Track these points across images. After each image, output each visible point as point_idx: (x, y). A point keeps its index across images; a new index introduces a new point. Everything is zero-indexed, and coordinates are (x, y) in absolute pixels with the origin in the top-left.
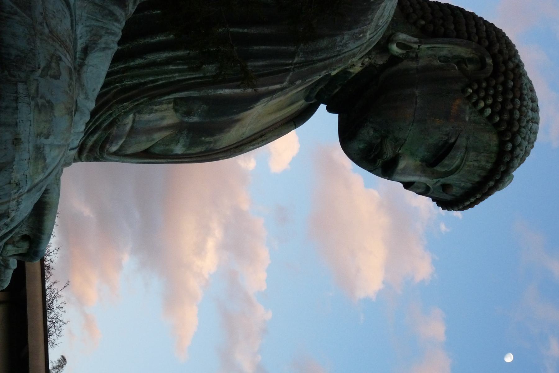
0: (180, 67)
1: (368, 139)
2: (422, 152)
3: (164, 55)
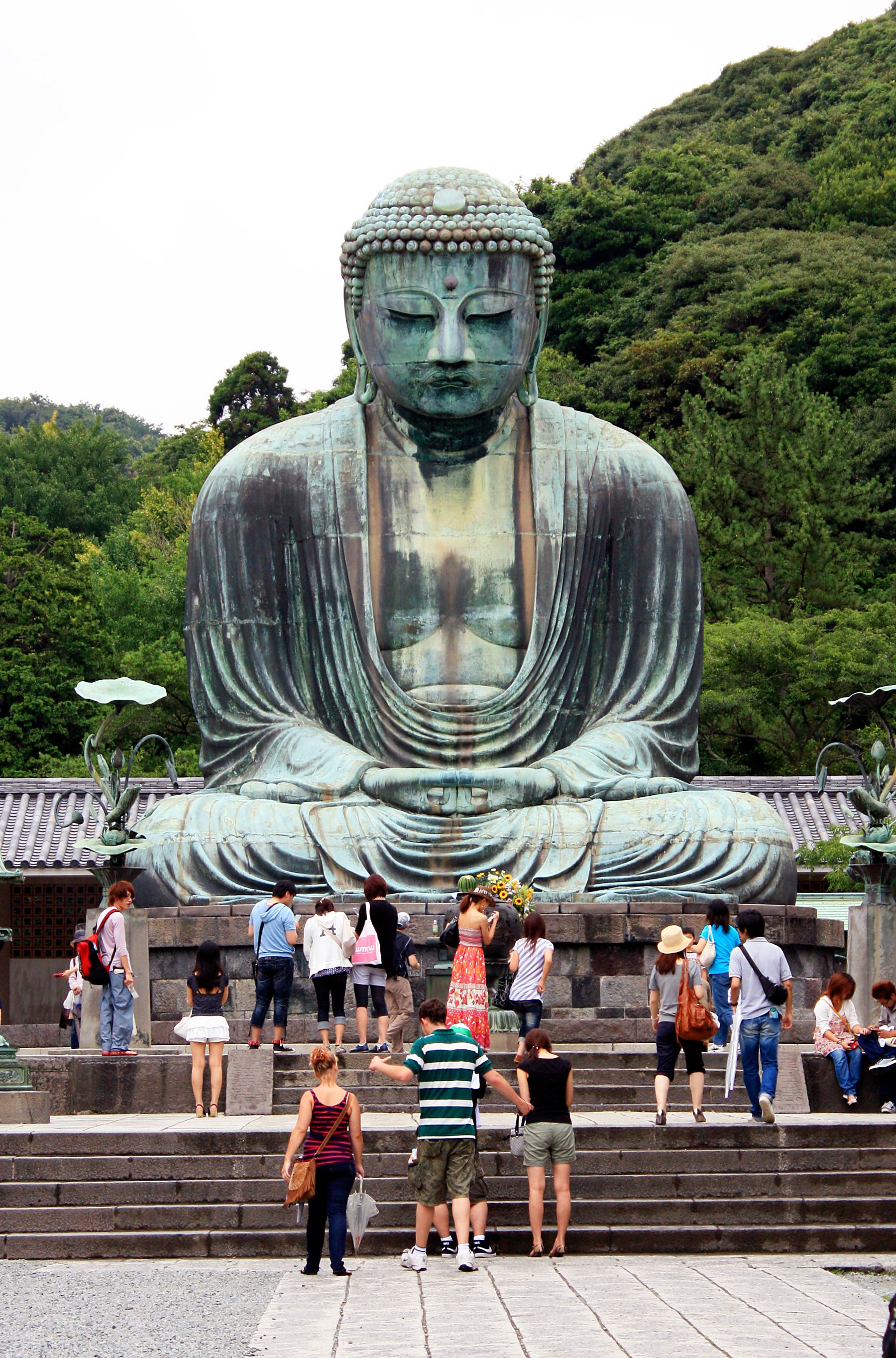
0: (348, 657)
1: (432, 400)
2: (415, 336)
3: (341, 676)
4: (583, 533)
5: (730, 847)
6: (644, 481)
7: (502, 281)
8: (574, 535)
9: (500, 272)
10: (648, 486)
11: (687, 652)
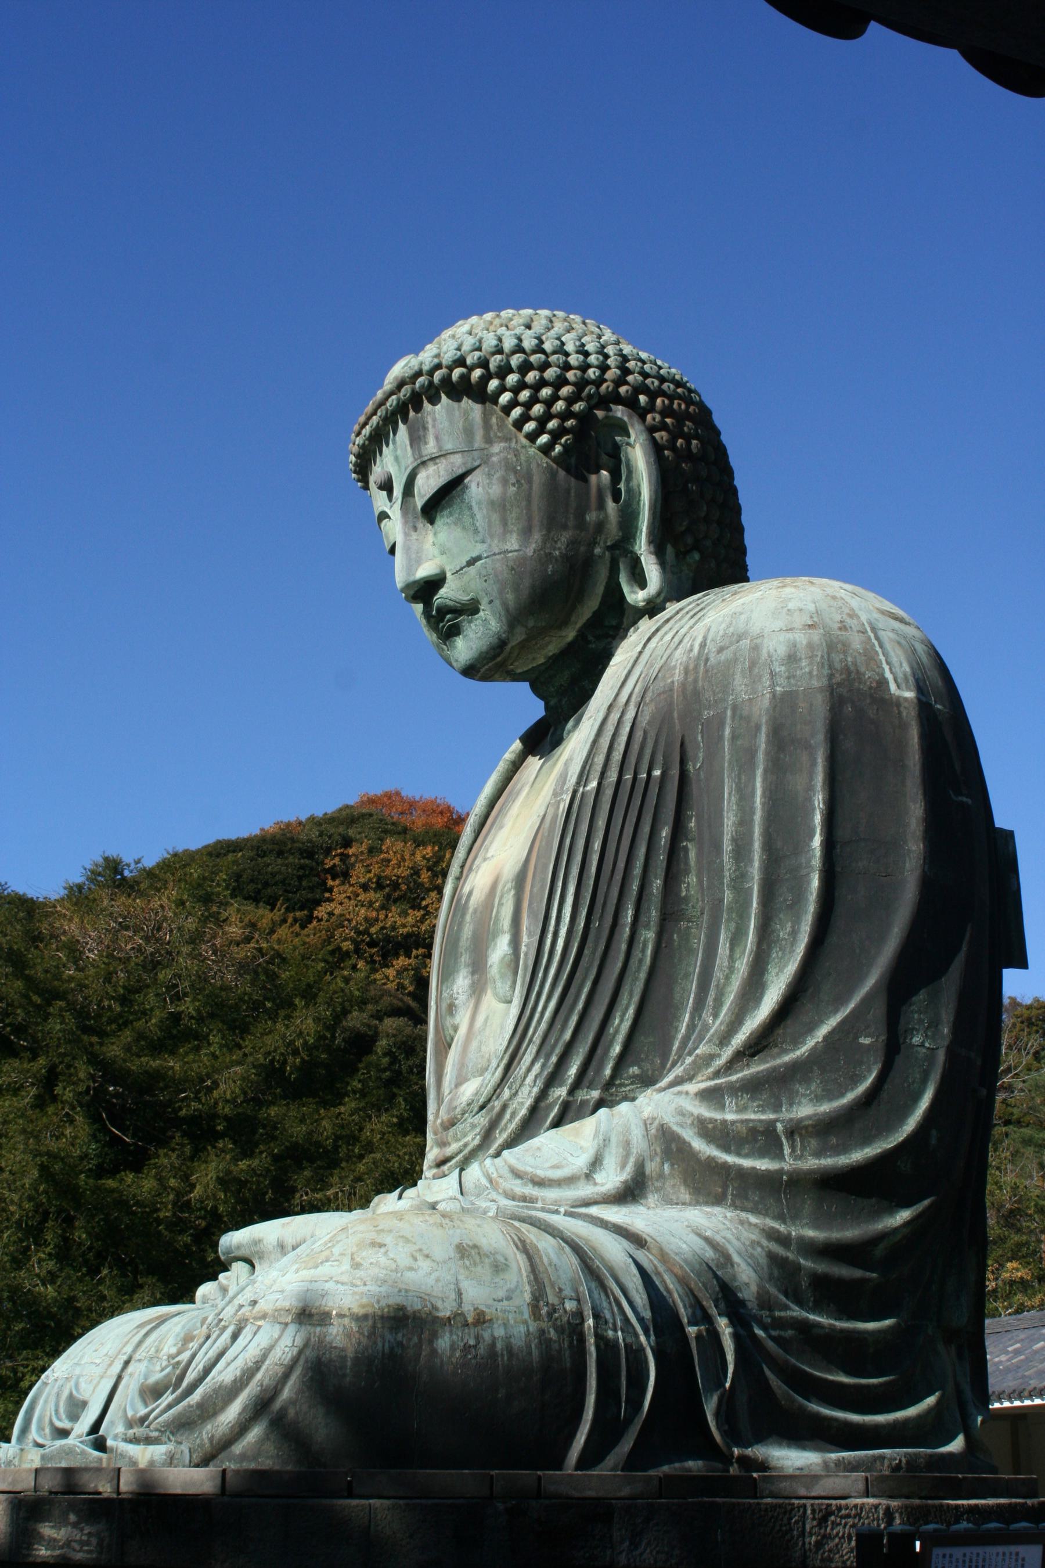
4: (613, 776)
5: (235, 1337)
6: (721, 650)
7: (426, 443)
8: (593, 784)
9: (421, 433)
10: (723, 657)
11: (794, 933)
